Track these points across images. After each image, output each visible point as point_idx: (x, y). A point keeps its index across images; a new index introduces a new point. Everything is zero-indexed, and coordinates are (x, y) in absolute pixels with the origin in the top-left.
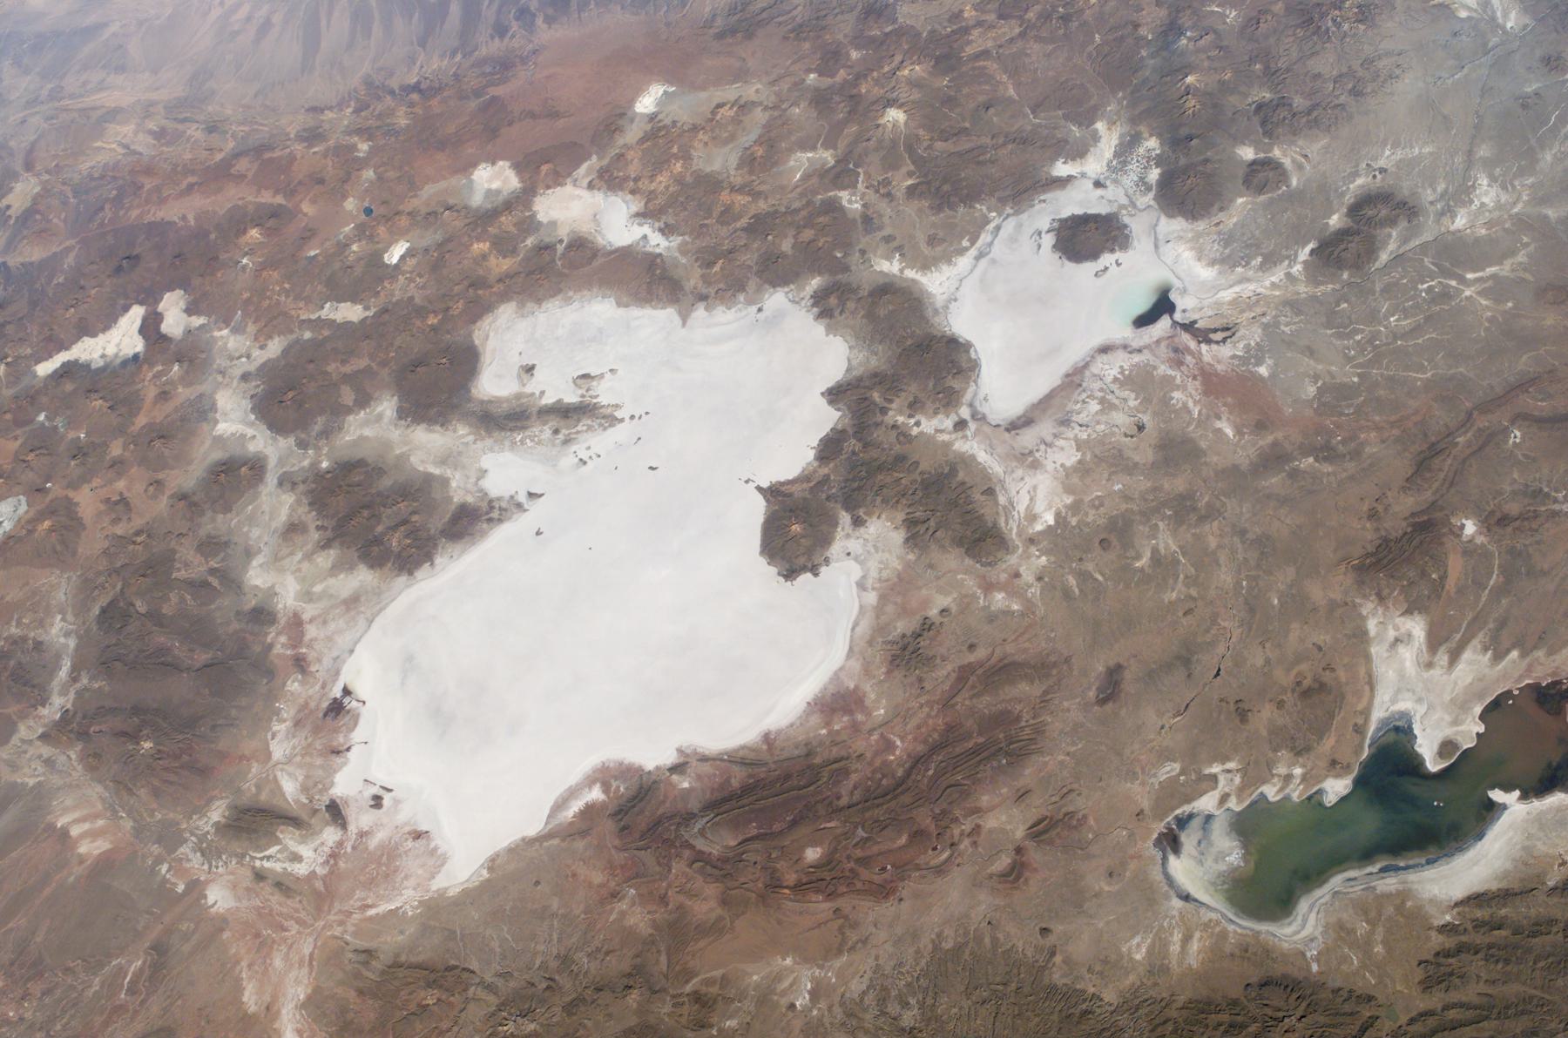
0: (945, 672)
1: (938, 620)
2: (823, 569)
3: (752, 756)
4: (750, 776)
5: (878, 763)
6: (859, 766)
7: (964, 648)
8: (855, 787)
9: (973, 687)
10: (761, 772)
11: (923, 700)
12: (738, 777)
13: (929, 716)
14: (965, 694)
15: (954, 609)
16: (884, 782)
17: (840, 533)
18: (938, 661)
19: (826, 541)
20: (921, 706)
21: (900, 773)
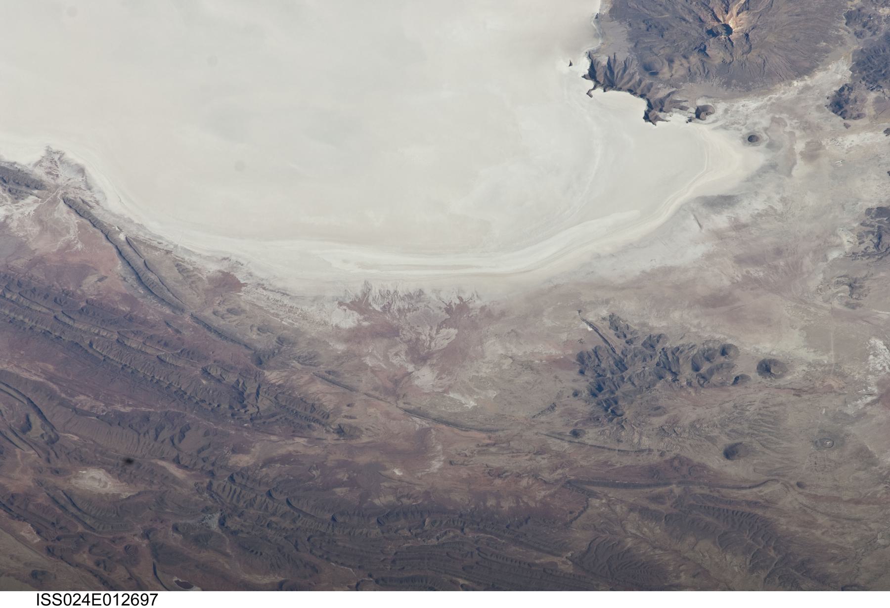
0: (646, 442)
1: (744, 366)
2: (676, 119)
3: (170, 275)
4: (128, 299)
5: (363, 459)
6: (331, 438)
7: (726, 441)
8: (285, 459)
9: (657, 499)
10: (154, 311)
11: (555, 445)
12: (110, 279)
13: (535, 475)
14: (631, 496)
15: (794, 376)
16: (339, 491)
17: (788, 91)
18: (658, 421)
19: (743, 78)
20: (541, 451)
21: (382, 501)
